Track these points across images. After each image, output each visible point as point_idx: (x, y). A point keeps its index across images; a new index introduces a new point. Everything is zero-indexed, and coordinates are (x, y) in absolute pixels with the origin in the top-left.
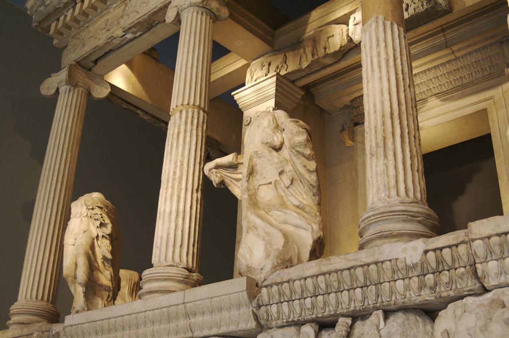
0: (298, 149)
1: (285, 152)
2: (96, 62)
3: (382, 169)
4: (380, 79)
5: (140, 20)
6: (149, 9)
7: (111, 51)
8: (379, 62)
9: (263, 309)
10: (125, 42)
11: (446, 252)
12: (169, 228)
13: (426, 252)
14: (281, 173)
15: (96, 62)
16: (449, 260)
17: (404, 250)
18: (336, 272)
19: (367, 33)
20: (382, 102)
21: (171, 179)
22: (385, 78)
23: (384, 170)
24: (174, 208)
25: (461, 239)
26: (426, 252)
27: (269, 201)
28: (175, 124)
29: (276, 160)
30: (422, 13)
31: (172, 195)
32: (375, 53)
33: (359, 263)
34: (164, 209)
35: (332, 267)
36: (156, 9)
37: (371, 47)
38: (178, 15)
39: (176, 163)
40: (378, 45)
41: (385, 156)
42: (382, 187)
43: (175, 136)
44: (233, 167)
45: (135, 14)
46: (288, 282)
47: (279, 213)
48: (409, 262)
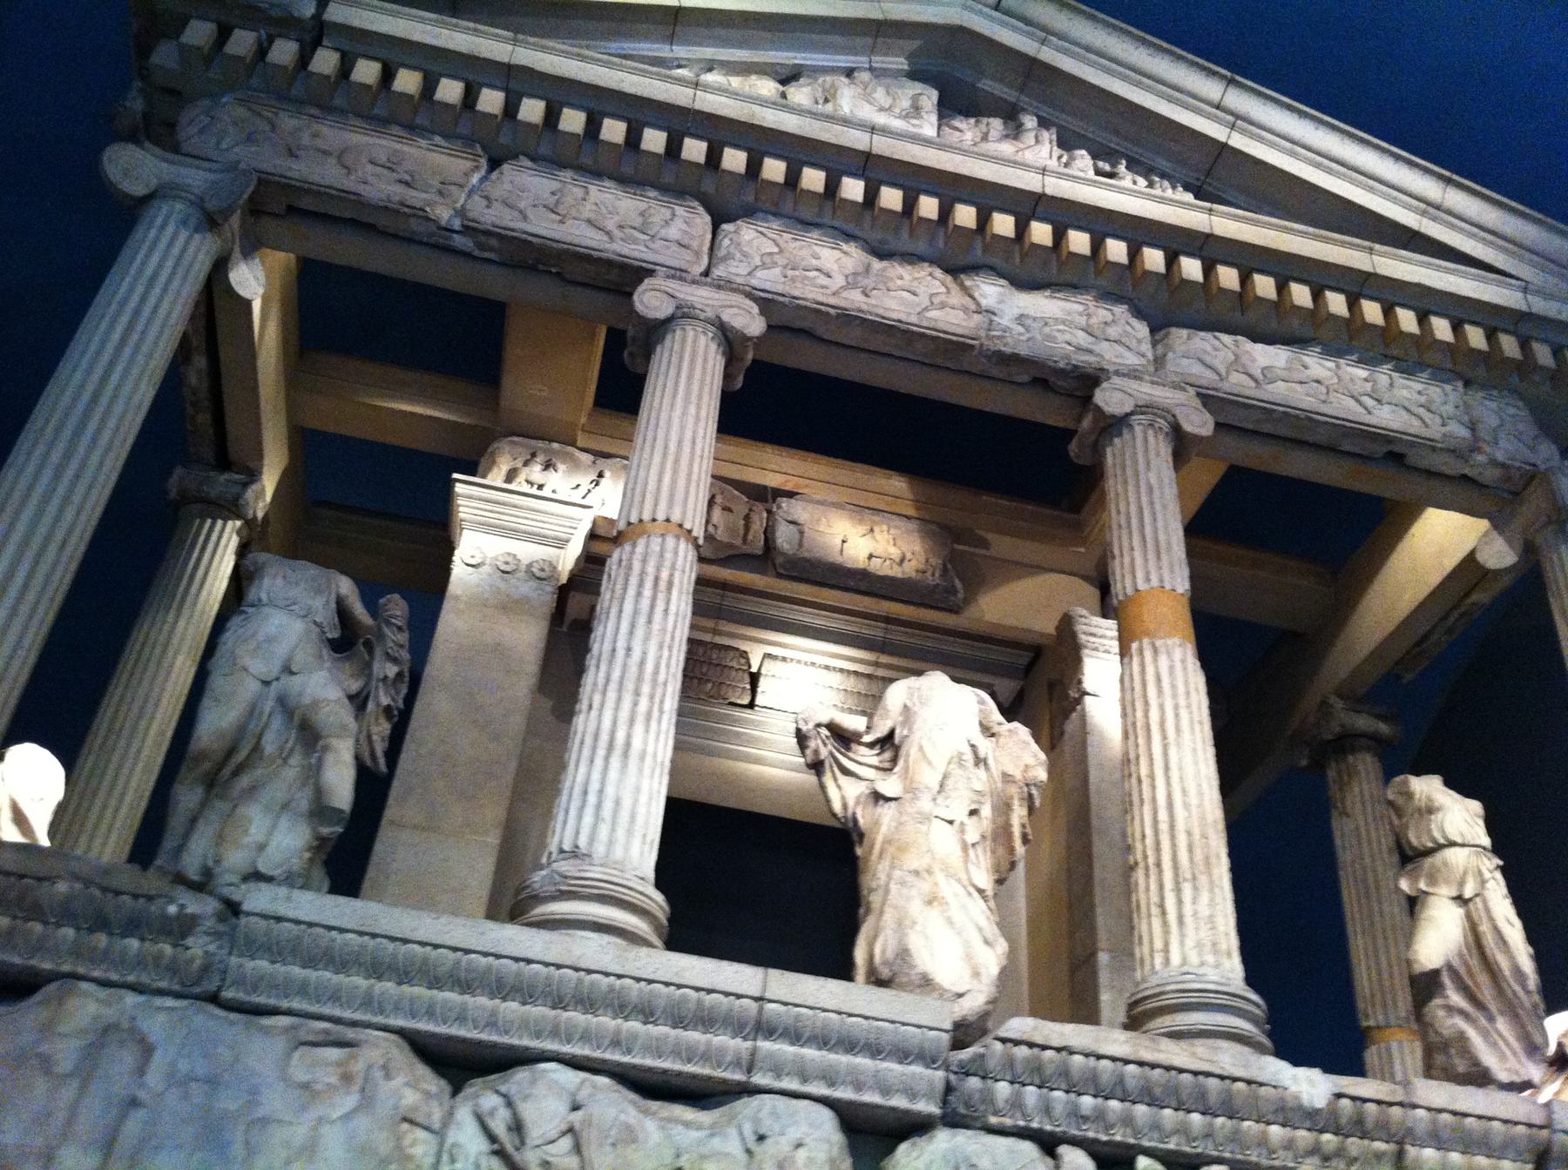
0: (1034, 792)
2: (292, 210)
3: (1207, 913)
4: (1195, 750)
6: (557, 236)
7: (371, 228)
9: (974, 1082)
10: (433, 240)
11: (1371, 1108)
12: (638, 790)
14: (973, 813)
15: (292, 210)
16: (1370, 1123)
18: (1168, 1068)
19: (1163, 662)
23: (1211, 916)
26: (1339, 1096)
28: (662, 556)
30: (928, 586)
33: (1218, 1071)
34: (629, 736)
36: (595, 254)
38: (670, 320)
40: (1188, 693)
41: (1211, 890)
45: (516, 214)
46: (1059, 1050)
48: (1306, 1100)
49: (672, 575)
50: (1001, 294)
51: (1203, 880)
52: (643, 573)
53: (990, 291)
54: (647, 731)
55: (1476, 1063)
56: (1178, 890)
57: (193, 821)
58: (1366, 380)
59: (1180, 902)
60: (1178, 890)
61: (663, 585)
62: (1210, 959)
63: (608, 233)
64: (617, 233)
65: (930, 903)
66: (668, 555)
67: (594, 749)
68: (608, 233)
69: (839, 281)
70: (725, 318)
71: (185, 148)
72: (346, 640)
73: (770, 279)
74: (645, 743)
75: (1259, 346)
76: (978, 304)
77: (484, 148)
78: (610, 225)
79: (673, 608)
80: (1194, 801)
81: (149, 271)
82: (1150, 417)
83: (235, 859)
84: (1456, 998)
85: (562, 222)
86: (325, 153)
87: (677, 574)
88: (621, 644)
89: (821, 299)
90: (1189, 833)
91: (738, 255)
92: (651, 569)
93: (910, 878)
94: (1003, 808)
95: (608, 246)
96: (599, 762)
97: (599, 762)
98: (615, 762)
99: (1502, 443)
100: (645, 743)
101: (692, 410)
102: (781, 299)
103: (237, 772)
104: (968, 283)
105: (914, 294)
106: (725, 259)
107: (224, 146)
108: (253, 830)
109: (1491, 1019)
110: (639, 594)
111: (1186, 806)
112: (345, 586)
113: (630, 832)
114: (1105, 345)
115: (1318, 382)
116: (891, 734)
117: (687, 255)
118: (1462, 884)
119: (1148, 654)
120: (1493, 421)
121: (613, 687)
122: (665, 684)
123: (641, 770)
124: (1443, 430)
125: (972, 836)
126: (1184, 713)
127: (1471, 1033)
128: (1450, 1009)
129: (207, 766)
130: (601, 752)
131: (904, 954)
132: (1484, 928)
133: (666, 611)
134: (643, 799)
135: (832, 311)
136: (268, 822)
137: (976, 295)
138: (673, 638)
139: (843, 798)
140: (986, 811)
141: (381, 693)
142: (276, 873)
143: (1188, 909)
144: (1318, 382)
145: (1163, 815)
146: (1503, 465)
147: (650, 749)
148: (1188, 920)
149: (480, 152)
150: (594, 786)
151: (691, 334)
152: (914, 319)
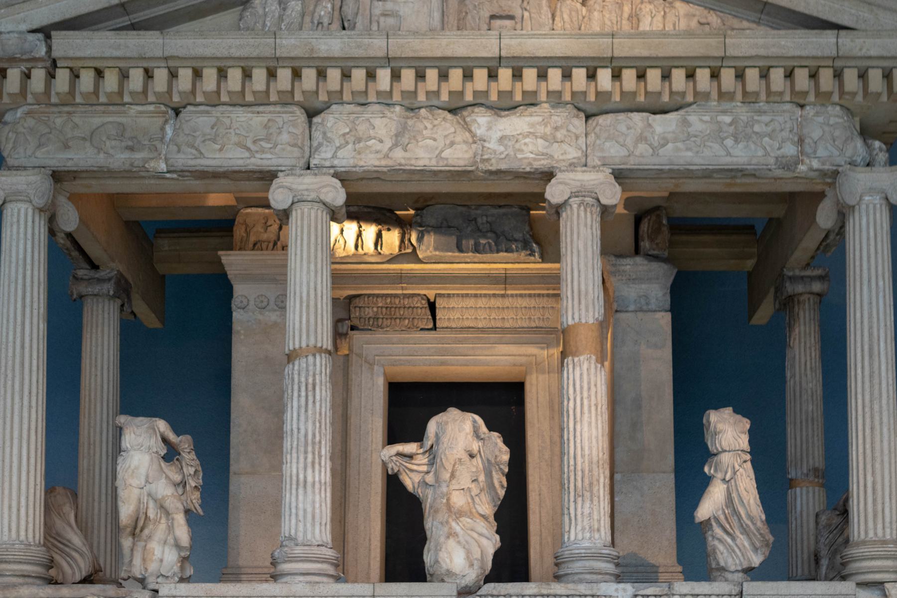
0: (502, 467)
1: (478, 461)
4: (590, 423)
5: (210, 169)
8: (590, 407)
12: (314, 502)
13: (636, 596)
17: (617, 590)
20: (590, 448)
21: (310, 441)
22: (593, 424)
24: (317, 479)
25: (665, 592)
27: (462, 507)
28: (307, 370)
29: (474, 470)
31: (313, 463)
32: (585, 394)
33: (578, 593)
34: (305, 477)
35: (552, 592)
36: (243, 169)
37: (582, 388)
38: (293, 203)
39: (314, 423)
40: (589, 389)
41: (592, 500)
42: (587, 528)
43: (310, 387)
44: (411, 457)
45: (194, 151)
47: (469, 520)
49: (314, 380)
50: (489, 123)
51: (587, 494)
52: (300, 382)
53: (481, 120)
54: (313, 472)
55: (718, 563)
56: (575, 501)
57: (132, 550)
58: (730, 124)
59: (576, 509)
60: (575, 501)
61: (310, 387)
62: (588, 535)
63: (248, 149)
64: (252, 147)
65: (448, 537)
66: (311, 368)
67: (291, 485)
68: (248, 149)
69: (388, 144)
70: (322, 197)
71: (10, 162)
72: (171, 454)
73: (346, 159)
74: (314, 477)
75: (658, 116)
76: (474, 136)
77: (165, 105)
78: (249, 144)
79: (318, 397)
80: (587, 452)
81: (21, 256)
82: (581, 198)
83: (153, 567)
84: (718, 531)
85: (221, 150)
86: (84, 139)
87: (317, 377)
88: (295, 426)
89: (377, 163)
90: (583, 471)
91: (325, 143)
92: (303, 379)
93: (440, 526)
94: (489, 475)
95: (248, 161)
96: (294, 492)
97: (294, 492)
98: (301, 491)
99: (821, 152)
100: (314, 477)
101: (312, 267)
102: (354, 169)
103: (141, 531)
104: (468, 119)
105: (435, 140)
106: (317, 149)
107: (29, 153)
108: (156, 553)
109: (733, 539)
110: (299, 396)
111: (583, 456)
112: (162, 425)
113: (313, 525)
114: (555, 145)
115: (696, 136)
116: (432, 447)
117: (296, 152)
118: (726, 473)
119: (571, 367)
120: (816, 134)
121: (294, 451)
122: (320, 442)
123: (314, 492)
124: (779, 153)
125: (475, 491)
126: (586, 402)
127: (721, 547)
128: (713, 537)
129: (129, 530)
130: (294, 486)
131: (437, 562)
132: (734, 495)
133: (314, 402)
134: (317, 505)
135: (385, 169)
136: (161, 548)
137: (473, 128)
138: (320, 414)
139: (413, 483)
140: (482, 478)
141: (191, 481)
142: (169, 574)
143: (579, 513)
144: (696, 136)
145: (572, 463)
146: (816, 170)
147: (317, 479)
148: (579, 516)
149: (163, 108)
150: (294, 505)
151: (306, 210)
152: (434, 162)
